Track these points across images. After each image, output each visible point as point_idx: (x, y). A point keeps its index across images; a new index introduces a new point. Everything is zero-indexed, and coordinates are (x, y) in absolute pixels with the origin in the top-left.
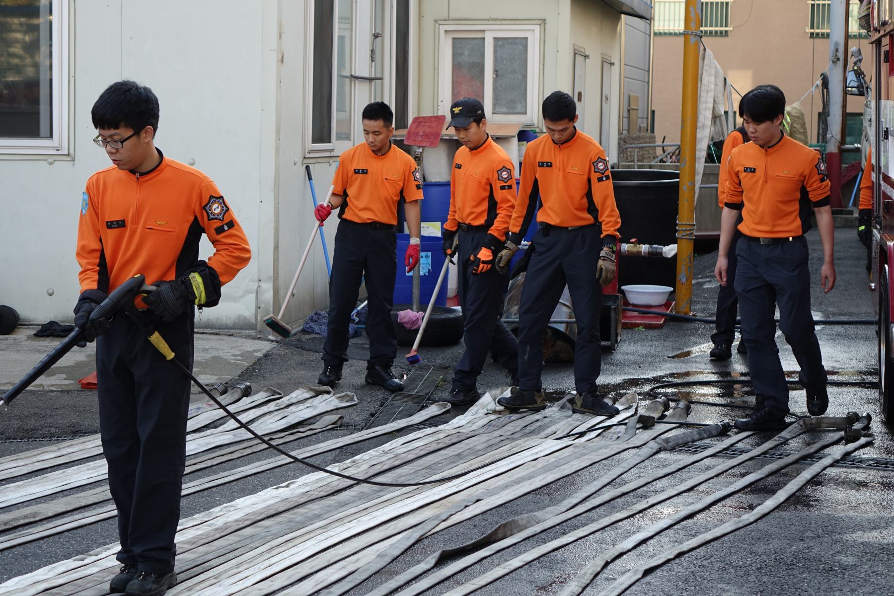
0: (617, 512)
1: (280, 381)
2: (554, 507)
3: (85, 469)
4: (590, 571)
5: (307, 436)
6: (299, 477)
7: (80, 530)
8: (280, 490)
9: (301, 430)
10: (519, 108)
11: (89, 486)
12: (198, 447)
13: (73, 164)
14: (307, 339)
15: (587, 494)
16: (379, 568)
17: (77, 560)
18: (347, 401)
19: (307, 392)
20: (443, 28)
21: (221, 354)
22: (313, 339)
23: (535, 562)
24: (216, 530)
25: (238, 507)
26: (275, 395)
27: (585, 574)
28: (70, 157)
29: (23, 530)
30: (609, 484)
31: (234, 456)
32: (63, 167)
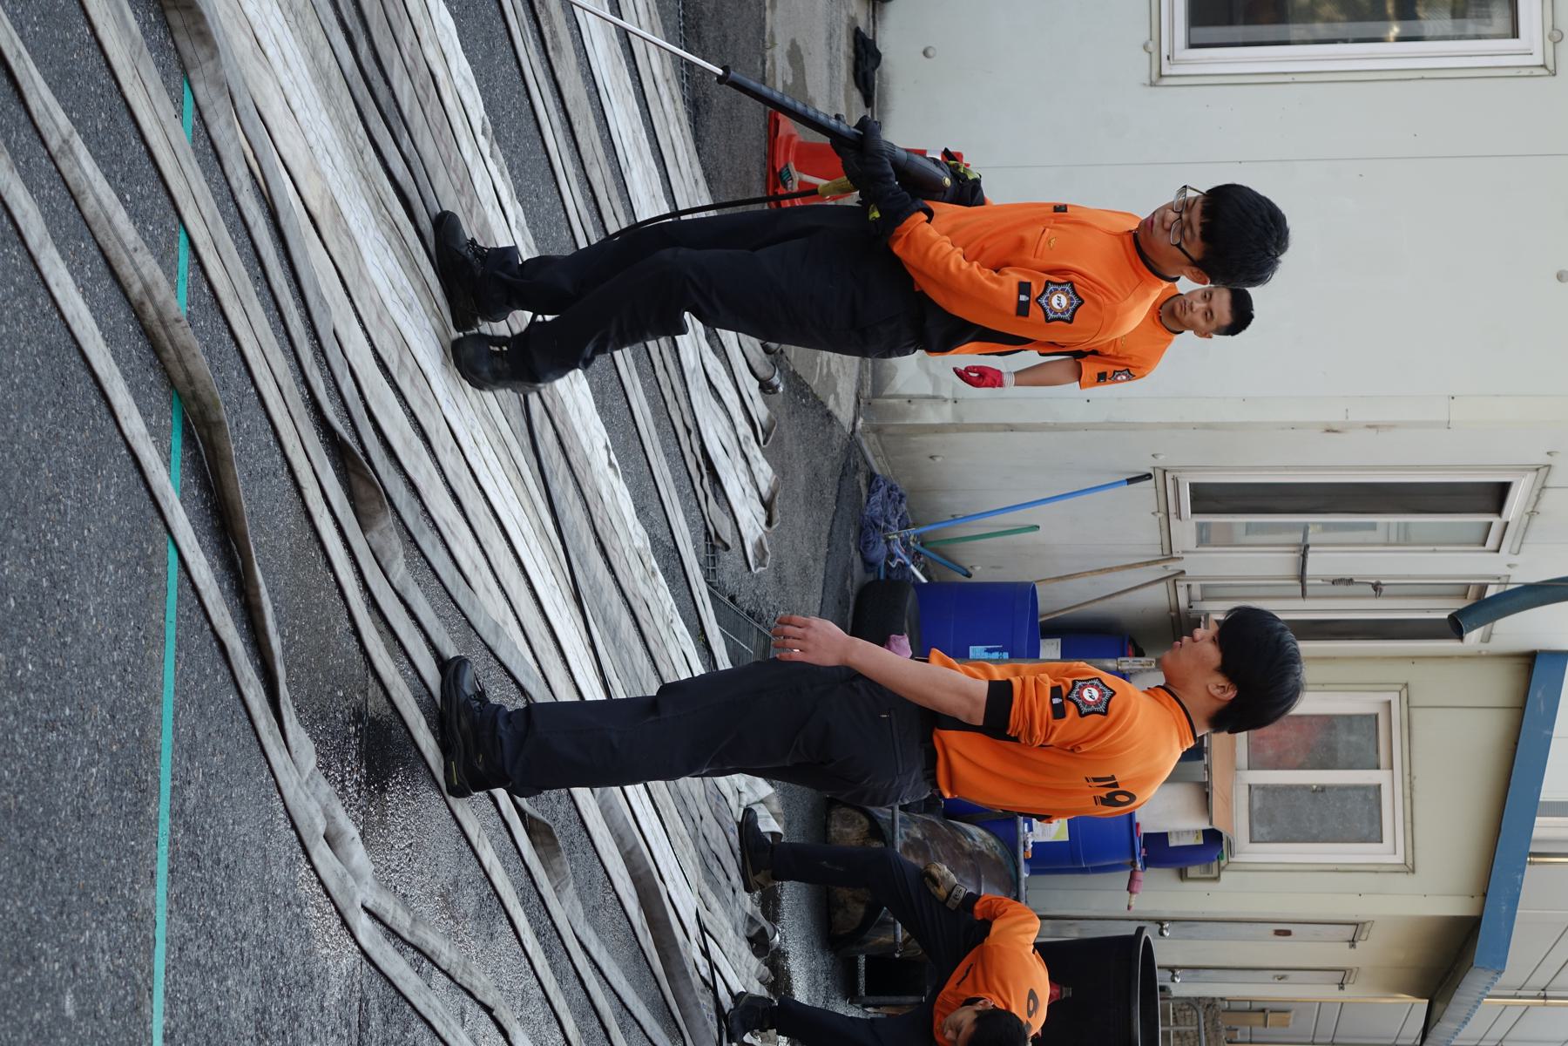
0: (575, 1021)
1: (786, 441)
2: (582, 915)
3: (635, 125)
4: (476, 982)
5: (695, 491)
6: (625, 482)
7: (532, 124)
8: (604, 453)
9: (706, 480)
10: (1261, 830)
11: (607, 135)
13: (1145, 84)
14: (858, 482)
15: (605, 969)
16: (476, 627)
17: (484, 123)
18: (755, 556)
19: (769, 488)
20: (1394, 697)
23: (489, 888)
25: (575, 386)
26: (766, 435)
27: (471, 974)
28: (1158, 79)
29: (532, 31)
30: (624, 1005)
31: (660, 373)
32: (1141, 66)
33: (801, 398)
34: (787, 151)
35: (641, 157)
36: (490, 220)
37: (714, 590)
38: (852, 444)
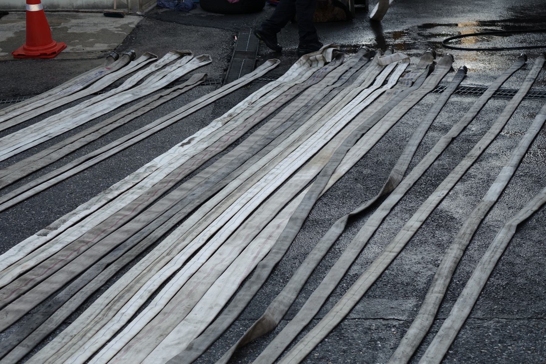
1: (152, 46)
3: (29, 132)
5: (186, 92)
6: (194, 133)
7: (36, 198)
9: (180, 86)
12: (109, 106)
14: (162, 12)
18: (204, 61)
19: (174, 54)
21: (106, 27)
22: (166, 12)
24: (148, 193)
25: (158, 166)
26: (153, 57)
31: (139, 113)
33: (133, 40)
34: (31, 50)
35: (43, 128)
36: (89, 229)
37: (225, 81)
38: (147, 16)
